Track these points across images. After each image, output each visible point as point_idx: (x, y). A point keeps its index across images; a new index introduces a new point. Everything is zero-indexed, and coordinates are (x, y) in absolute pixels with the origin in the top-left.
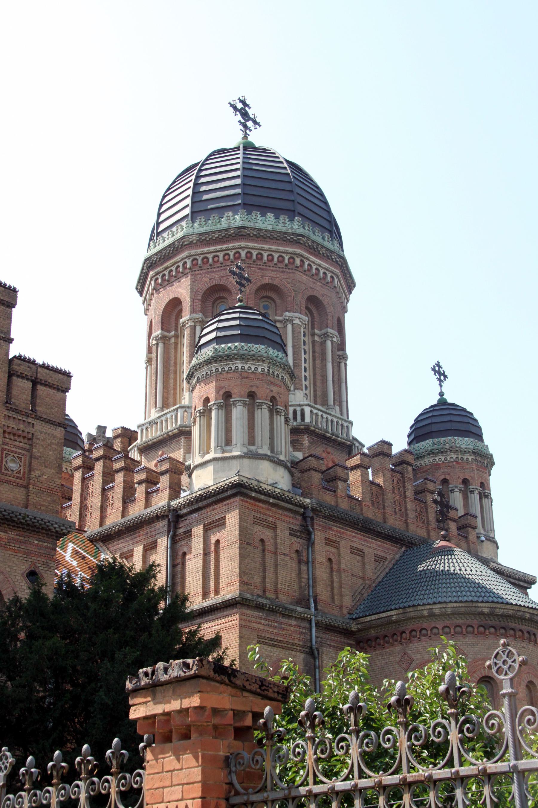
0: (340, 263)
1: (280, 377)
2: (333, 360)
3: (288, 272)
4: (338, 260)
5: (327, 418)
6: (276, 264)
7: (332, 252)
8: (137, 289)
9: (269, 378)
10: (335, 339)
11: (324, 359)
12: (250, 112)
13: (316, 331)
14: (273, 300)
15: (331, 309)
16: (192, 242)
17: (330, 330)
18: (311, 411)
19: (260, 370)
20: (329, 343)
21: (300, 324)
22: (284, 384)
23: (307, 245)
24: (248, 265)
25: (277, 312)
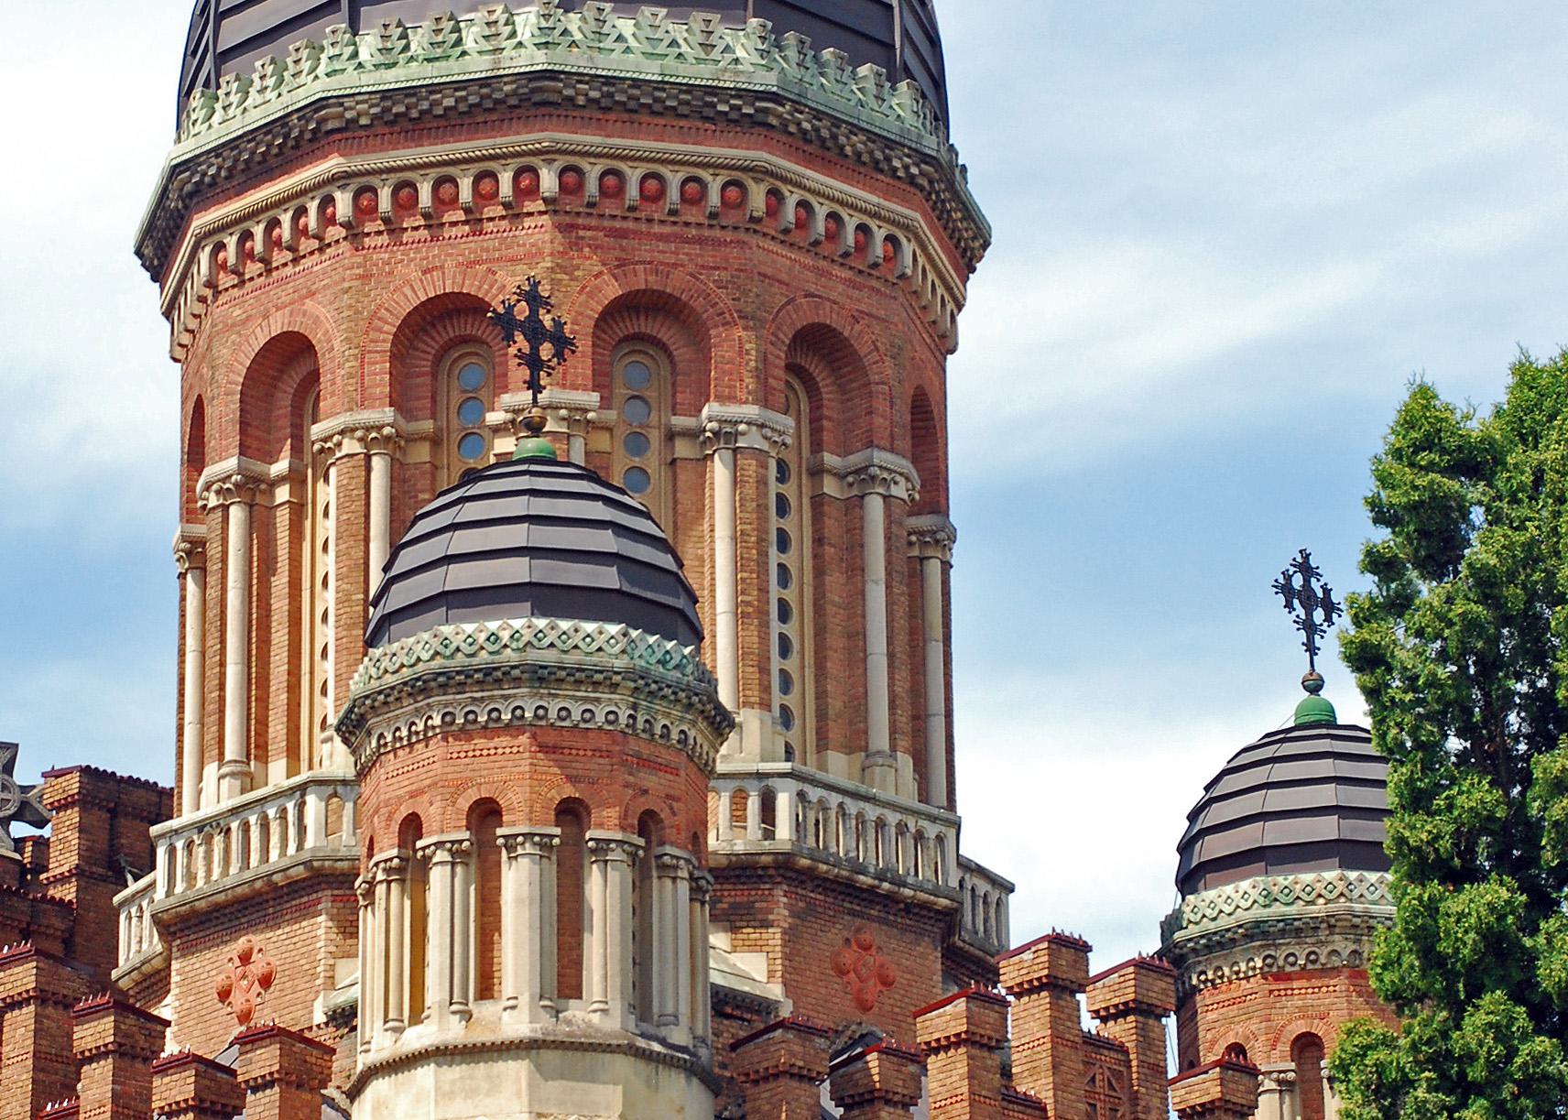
0: (925, 183)
1: (675, 736)
2: (889, 573)
4: (914, 170)
5: (860, 816)
6: (672, 212)
7: (889, 144)
8: (138, 253)
10: (900, 491)
11: (856, 569)
13: (830, 459)
14: (663, 347)
15: (888, 368)
16: (354, 121)
17: (881, 457)
18: (801, 796)
19: (600, 718)
20: (875, 507)
21: (765, 446)
22: (690, 758)
23: (792, 129)
24: (567, 219)
25: (679, 397)
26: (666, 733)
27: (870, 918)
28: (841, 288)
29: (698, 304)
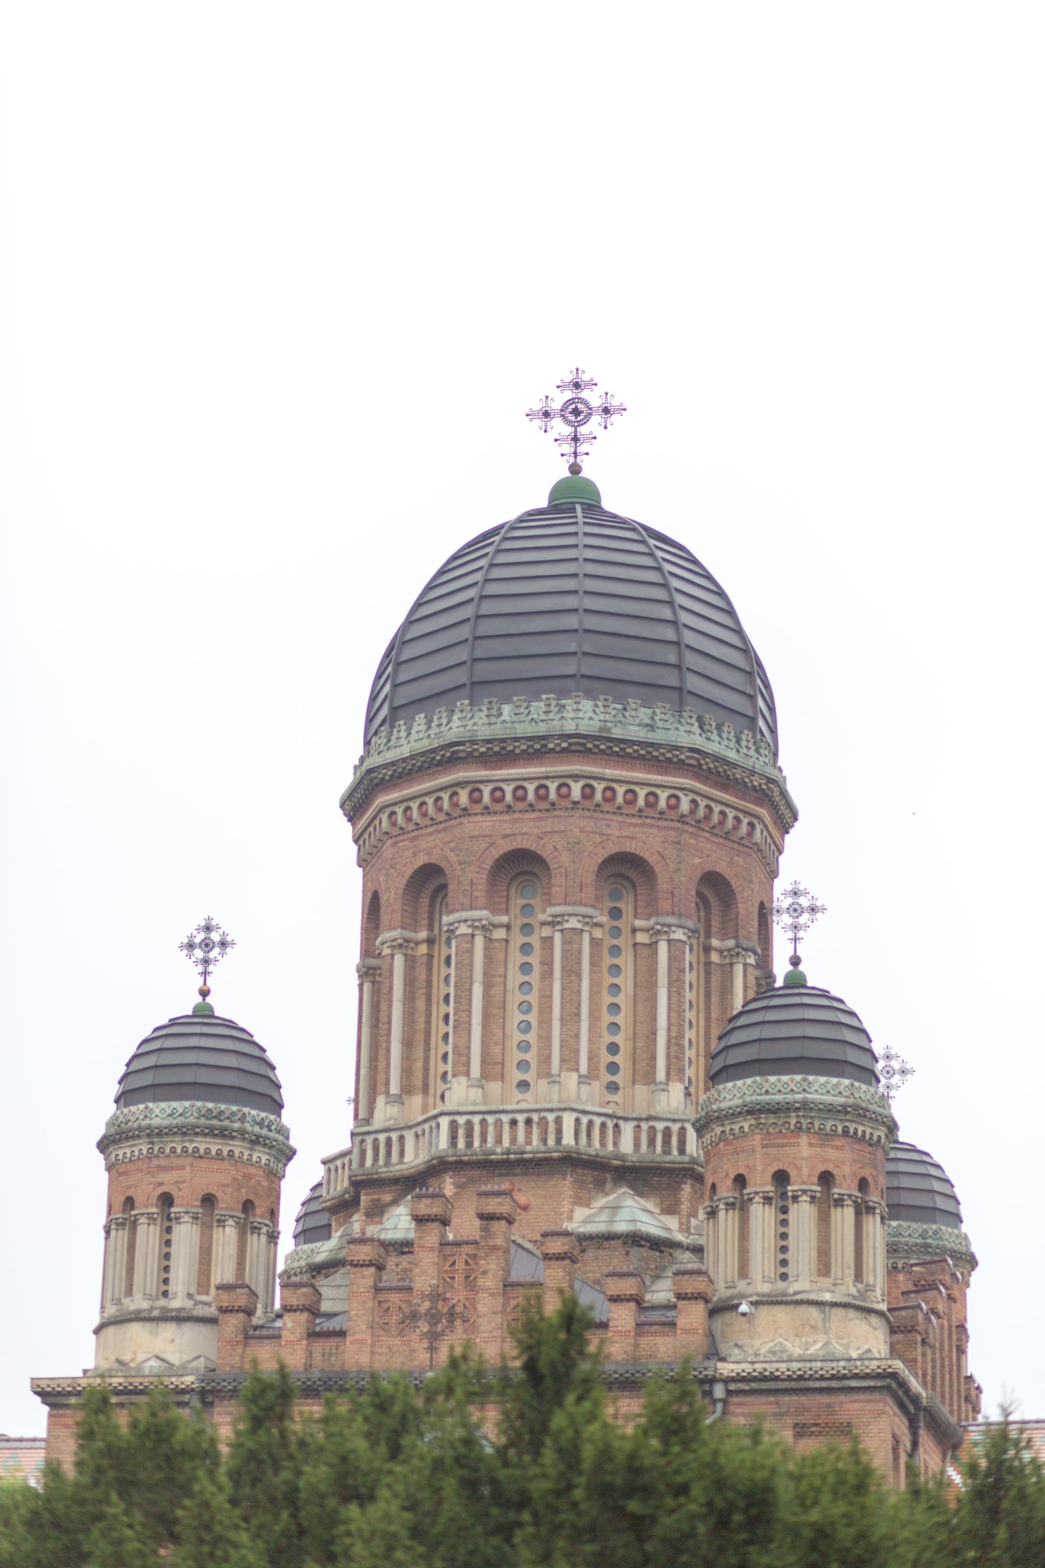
1: (179, 1151)
3: (452, 827)
9: (155, 1162)
10: (573, 923)
12: (593, 397)
15: (565, 858)
18: (454, 1126)
24: (394, 840)
26: (173, 1150)
27: (515, 1175)
28: (530, 824)
29: (442, 865)
